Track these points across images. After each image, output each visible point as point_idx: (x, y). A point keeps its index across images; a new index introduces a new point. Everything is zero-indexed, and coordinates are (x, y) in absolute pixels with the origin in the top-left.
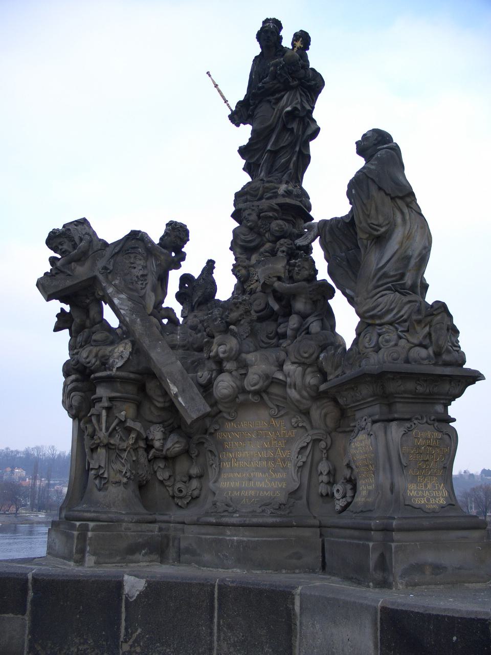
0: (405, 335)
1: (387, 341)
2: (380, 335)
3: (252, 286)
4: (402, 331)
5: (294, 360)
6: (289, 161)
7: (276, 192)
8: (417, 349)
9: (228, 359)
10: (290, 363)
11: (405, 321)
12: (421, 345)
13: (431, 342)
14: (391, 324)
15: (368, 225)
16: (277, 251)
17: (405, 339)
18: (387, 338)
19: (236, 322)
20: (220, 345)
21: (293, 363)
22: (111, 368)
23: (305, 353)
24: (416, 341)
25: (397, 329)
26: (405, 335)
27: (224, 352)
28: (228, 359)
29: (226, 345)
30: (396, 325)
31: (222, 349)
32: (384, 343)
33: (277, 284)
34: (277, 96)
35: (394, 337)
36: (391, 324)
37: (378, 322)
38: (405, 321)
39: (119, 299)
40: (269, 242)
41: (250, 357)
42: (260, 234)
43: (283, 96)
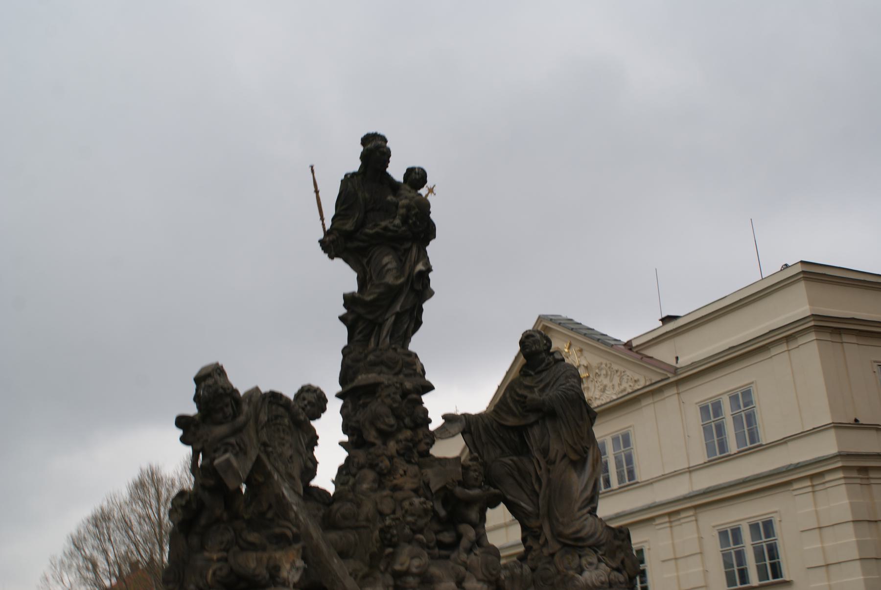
0: (603, 559)
1: (591, 564)
2: (580, 557)
3: (395, 482)
4: (602, 555)
5: (480, 576)
6: (408, 327)
7: (415, 370)
8: (616, 573)
9: (414, 575)
10: (475, 580)
11: (603, 545)
12: (618, 570)
13: (624, 567)
14: (590, 547)
15: (582, 447)
16: (420, 441)
17: (604, 563)
18: (590, 560)
19: (421, 531)
20: (412, 558)
21: (479, 580)
22: (287, 584)
23: (494, 569)
24: (614, 565)
25: (596, 552)
26: (603, 559)
27: (418, 567)
28: (414, 575)
29: (420, 559)
30: (596, 549)
31: (416, 562)
32: (588, 566)
33: (458, 490)
34: (407, 245)
35: (594, 560)
36: (590, 547)
37: (580, 544)
38: (603, 545)
39: (285, 488)
40: (406, 427)
41: (435, 570)
42: (398, 417)
43: (410, 249)
